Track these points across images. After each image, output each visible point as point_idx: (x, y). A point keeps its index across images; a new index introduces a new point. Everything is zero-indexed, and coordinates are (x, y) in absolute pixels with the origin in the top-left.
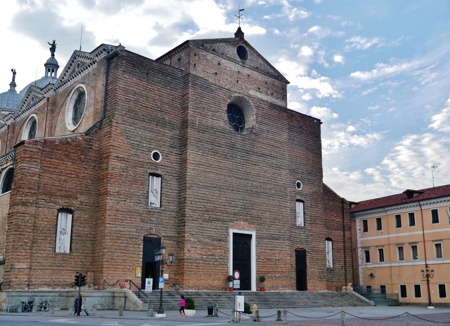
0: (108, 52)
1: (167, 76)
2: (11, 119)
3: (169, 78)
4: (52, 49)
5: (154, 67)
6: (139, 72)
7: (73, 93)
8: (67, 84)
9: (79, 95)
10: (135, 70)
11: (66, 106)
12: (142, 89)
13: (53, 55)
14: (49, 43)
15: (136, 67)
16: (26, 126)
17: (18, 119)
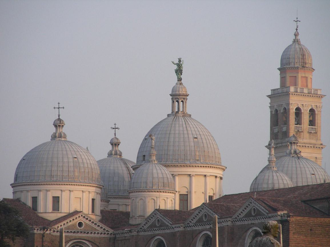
0: (282, 217)
1: (326, 227)
2: (181, 228)
3: (327, 228)
4: (178, 71)
5: (316, 223)
6: (304, 231)
7: (251, 232)
8: (244, 221)
9: (255, 233)
10: (301, 229)
11: (244, 239)
12: (307, 243)
13: (180, 79)
14: (173, 62)
15: (303, 227)
16: (200, 239)
17: (189, 229)
